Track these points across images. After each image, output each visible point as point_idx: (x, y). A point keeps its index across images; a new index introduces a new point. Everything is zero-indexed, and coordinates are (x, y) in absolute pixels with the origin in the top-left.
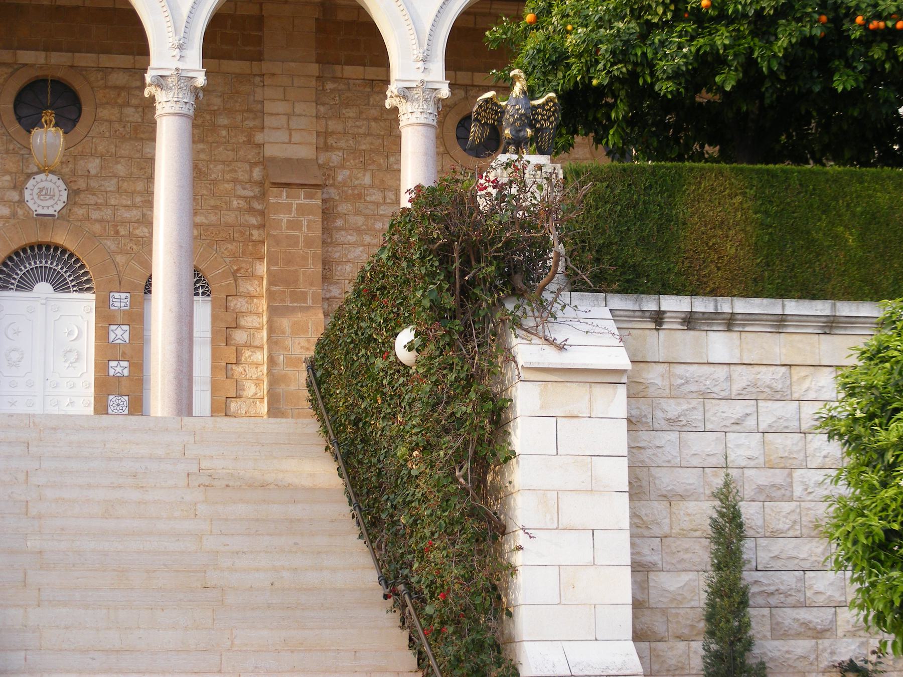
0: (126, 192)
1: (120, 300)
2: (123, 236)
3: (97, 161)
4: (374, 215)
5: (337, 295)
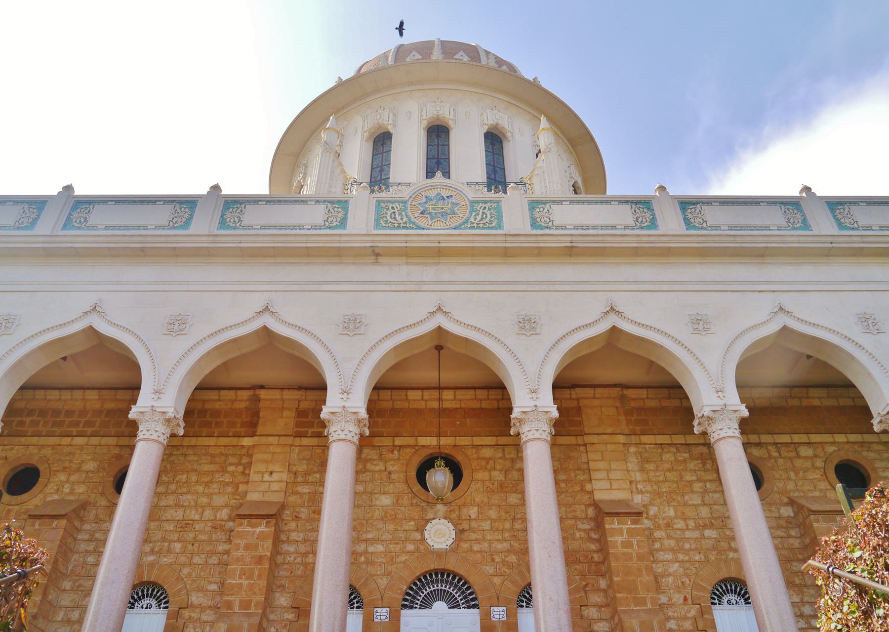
0: (497, 530)
1: (498, 613)
3: (476, 509)
5: (665, 602)
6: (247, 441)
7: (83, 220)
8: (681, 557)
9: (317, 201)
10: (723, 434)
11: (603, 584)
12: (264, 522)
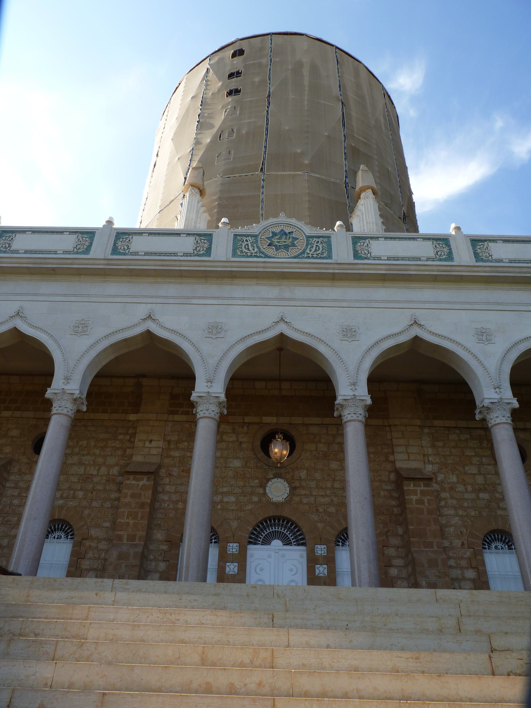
0: (321, 488)
1: (321, 550)
2: (321, 512)
4: (462, 499)
6: (132, 417)
7: (7, 246)
8: (460, 512)
9: (189, 234)
10: (498, 421)
11: (400, 530)
12: (145, 478)
